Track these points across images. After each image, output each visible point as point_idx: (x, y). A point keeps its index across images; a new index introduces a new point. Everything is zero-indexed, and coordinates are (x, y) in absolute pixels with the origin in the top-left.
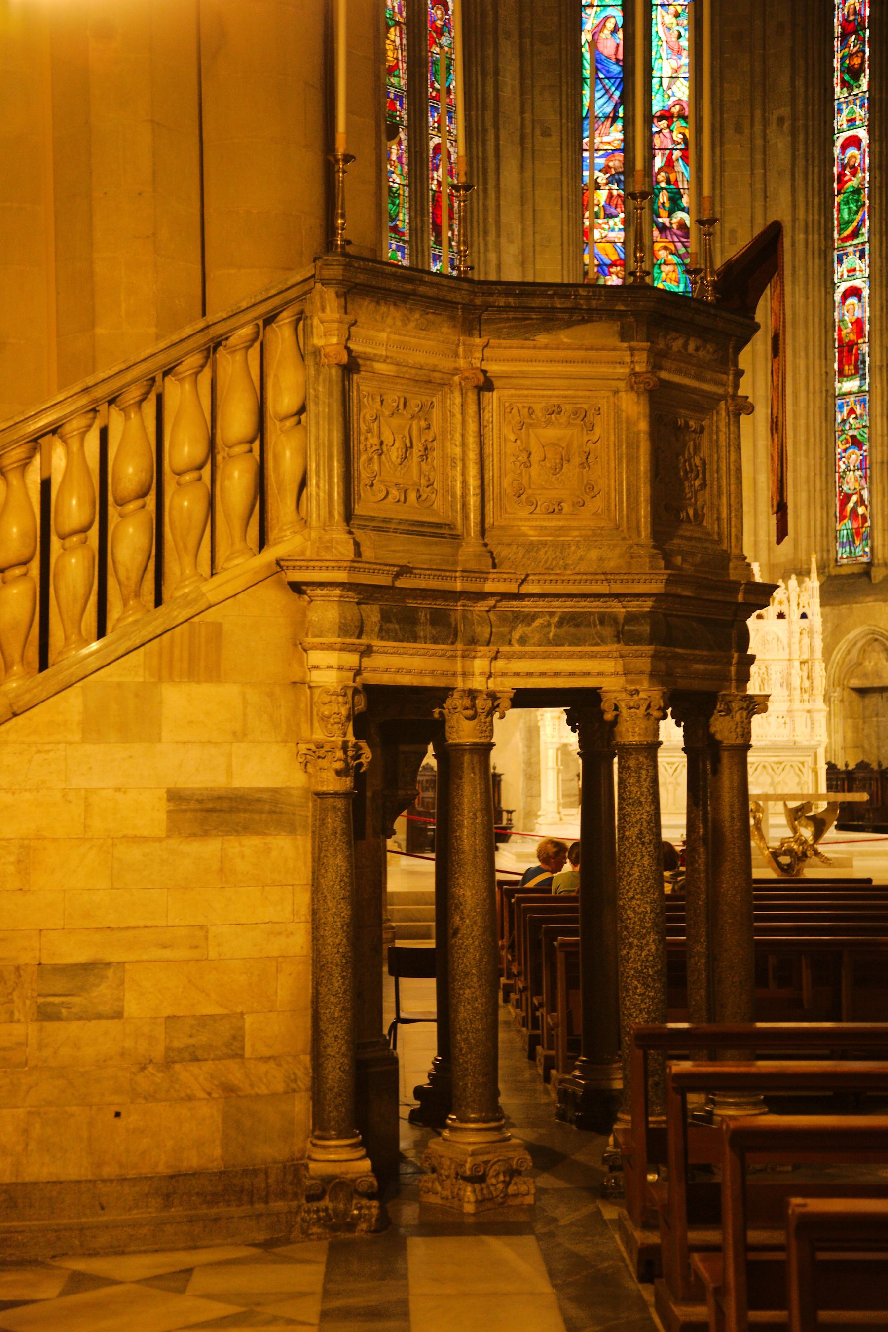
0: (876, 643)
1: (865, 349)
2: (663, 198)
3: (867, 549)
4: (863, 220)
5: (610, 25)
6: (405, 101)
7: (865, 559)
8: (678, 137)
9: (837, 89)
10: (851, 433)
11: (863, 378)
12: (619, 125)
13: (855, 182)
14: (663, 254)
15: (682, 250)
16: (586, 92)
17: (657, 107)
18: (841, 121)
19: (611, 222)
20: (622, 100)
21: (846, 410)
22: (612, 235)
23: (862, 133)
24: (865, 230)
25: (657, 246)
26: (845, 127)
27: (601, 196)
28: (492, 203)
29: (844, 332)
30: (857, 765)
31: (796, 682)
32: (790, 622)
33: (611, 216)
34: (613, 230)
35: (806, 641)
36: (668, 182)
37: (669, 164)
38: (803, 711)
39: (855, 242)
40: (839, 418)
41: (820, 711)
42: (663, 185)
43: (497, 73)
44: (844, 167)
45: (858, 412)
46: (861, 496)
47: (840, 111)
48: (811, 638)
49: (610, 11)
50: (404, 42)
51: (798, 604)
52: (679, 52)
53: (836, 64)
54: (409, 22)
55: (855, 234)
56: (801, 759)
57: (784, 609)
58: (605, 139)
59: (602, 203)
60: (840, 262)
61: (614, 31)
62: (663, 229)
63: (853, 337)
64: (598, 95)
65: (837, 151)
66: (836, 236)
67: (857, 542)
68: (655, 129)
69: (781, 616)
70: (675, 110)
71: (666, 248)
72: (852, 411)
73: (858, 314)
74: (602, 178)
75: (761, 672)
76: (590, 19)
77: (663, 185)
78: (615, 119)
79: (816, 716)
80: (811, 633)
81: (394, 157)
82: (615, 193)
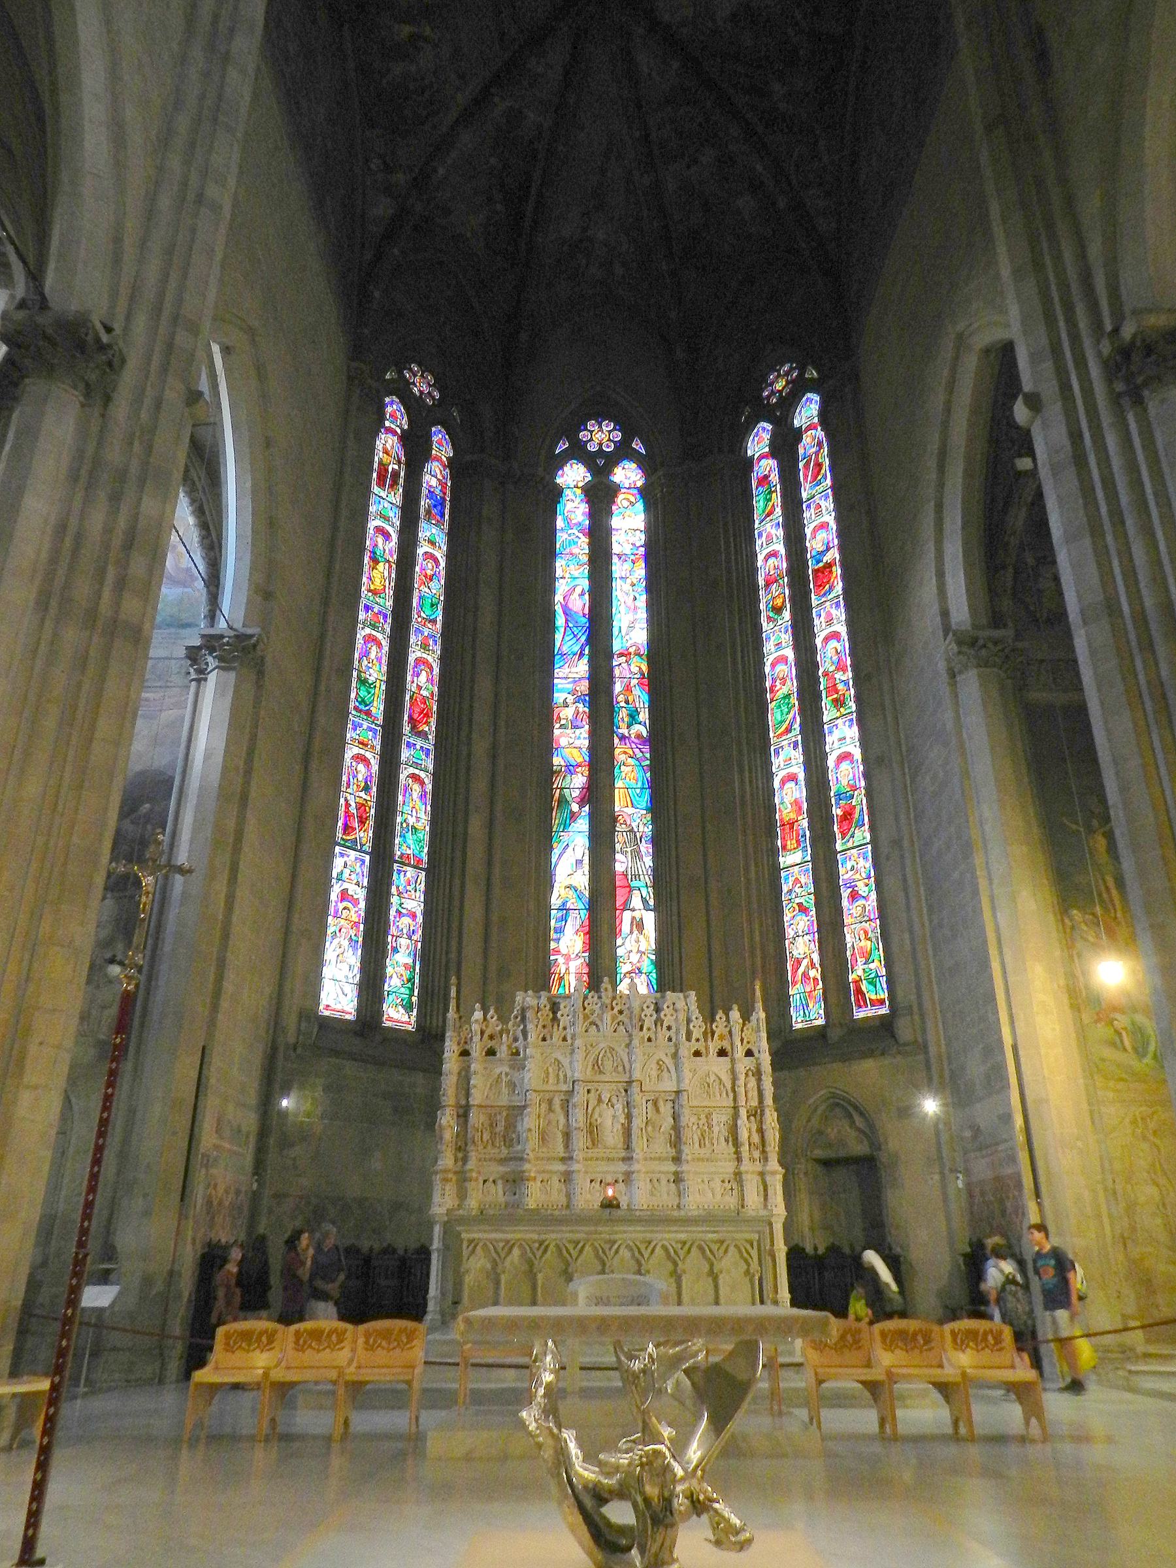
0: (837, 1110)
1: (805, 823)
2: (623, 713)
3: (822, 1012)
4: (795, 718)
5: (578, 590)
6: (389, 620)
7: (821, 1022)
8: (635, 669)
9: (764, 624)
10: (798, 900)
11: (805, 850)
12: (585, 659)
13: (785, 690)
14: (622, 757)
15: (639, 755)
16: (558, 636)
17: (617, 646)
18: (769, 647)
19: (578, 731)
20: (588, 641)
21: (791, 880)
22: (577, 743)
23: (790, 653)
24: (797, 726)
25: (617, 751)
26: (773, 650)
27: (568, 713)
28: (466, 706)
29: (785, 812)
30: (827, 1249)
31: (744, 1135)
32: (733, 1061)
33: (577, 727)
34: (579, 738)
35: (752, 1083)
36: (627, 702)
37: (628, 689)
38: (753, 1173)
39: (790, 735)
40: (785, 889)
41: (774, 1173)
42: (623, 704)
43: (477, 609)
44: (774, 680)
45: (803, 881)
46: (812, 960)
47: (768, 639)
48: (759, 1080)
49: (577, 582)
50: (393, 575)
51: (742, 1040)
52: (635, 608)
53: (762, 606)
54: (399, 563)
55: (788, 730)
56: (747, 1236)
57: (726, 1044)
58: (574, 670)
59: (570, 717)
60: (777, 753)
61: (582, 594)
62: (623, 738)
63: (793, 816)
64: (567, 638)
65: (767, 669)
66: (771, 735)
67: (811, 1006)
68: (615, 663)
69: (722, 1053)
70: (632, 650)
71: (625, 753)
72: (797, 881)
73: (797, 795)
74: (570, 699)
75: (701, 1123)
76: (561, 588)
77: (623, 704)
78: (581, 655)
79: (768, 1178)
80: (758, 1074)
81: (373, 655)
82: (581, 710)
